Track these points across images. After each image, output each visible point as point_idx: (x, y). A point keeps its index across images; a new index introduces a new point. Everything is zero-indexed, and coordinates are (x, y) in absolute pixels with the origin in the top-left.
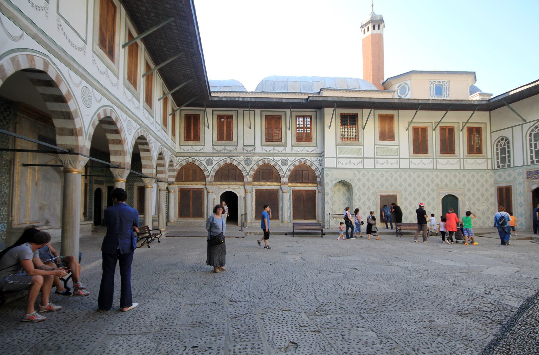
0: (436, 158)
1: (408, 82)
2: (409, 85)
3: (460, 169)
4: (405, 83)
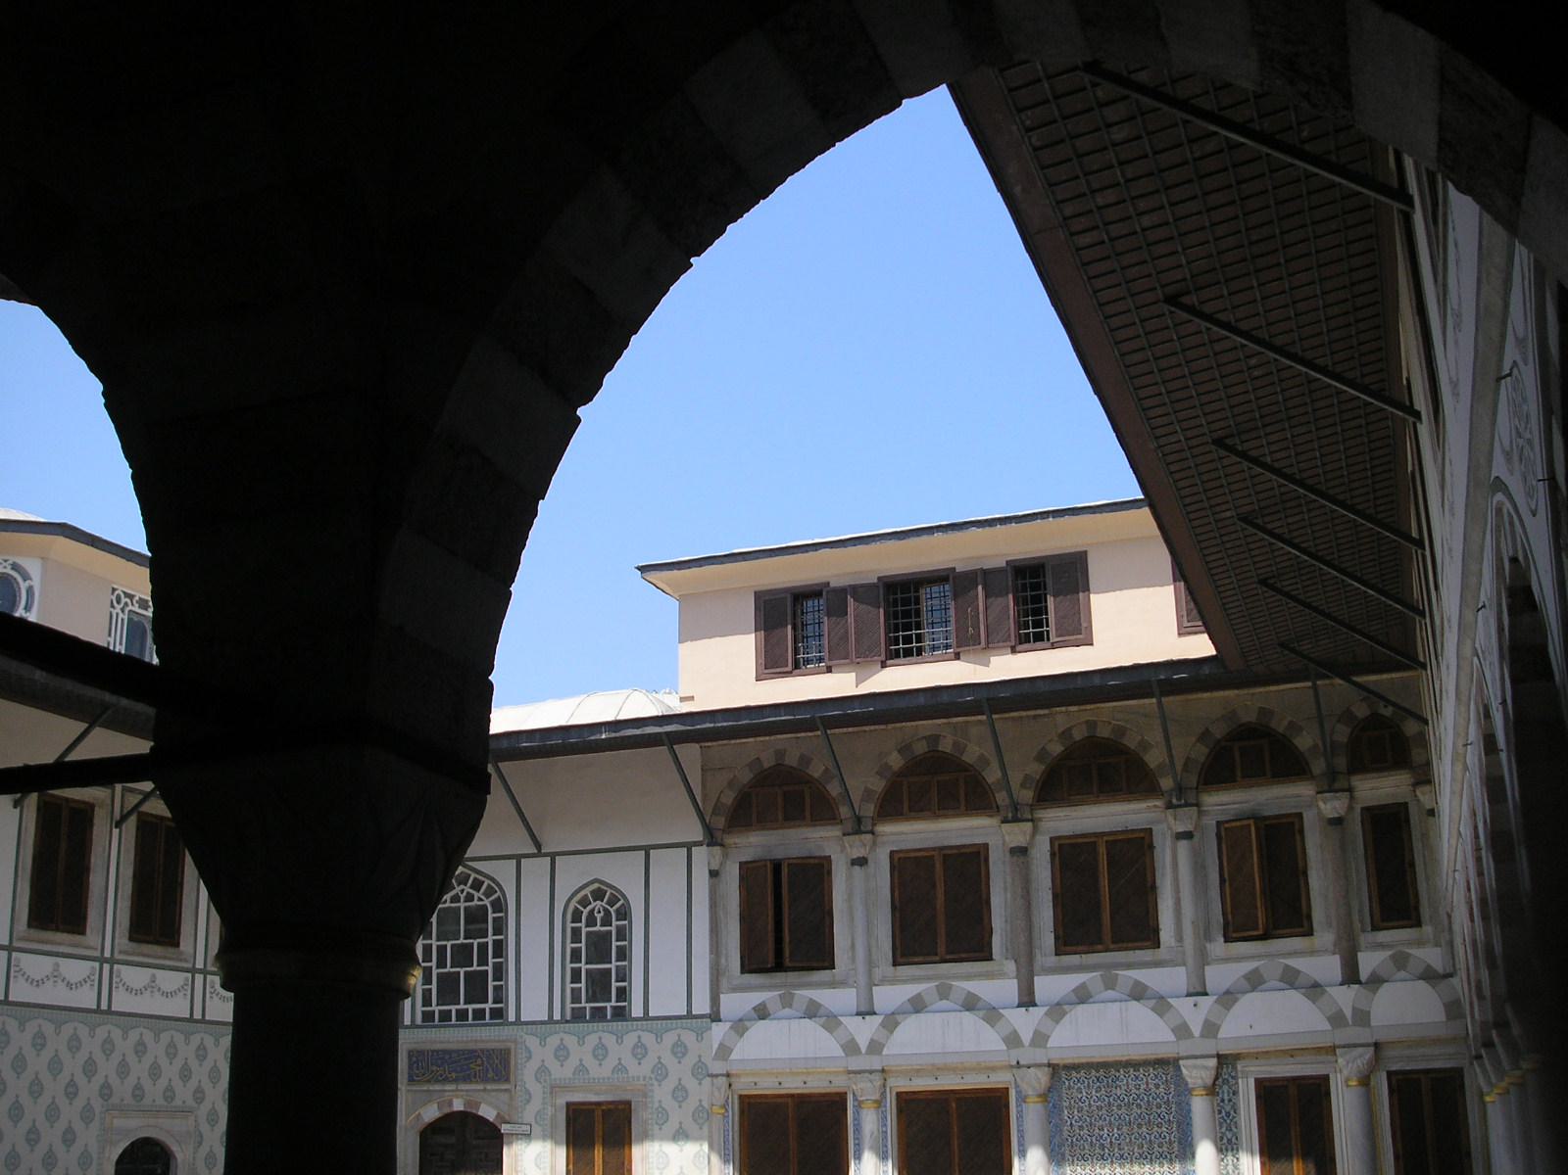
0: (112, 961)
1: (33, 567)
2: (36, 583)
3: (191, 1020)
4: (15, 567)
